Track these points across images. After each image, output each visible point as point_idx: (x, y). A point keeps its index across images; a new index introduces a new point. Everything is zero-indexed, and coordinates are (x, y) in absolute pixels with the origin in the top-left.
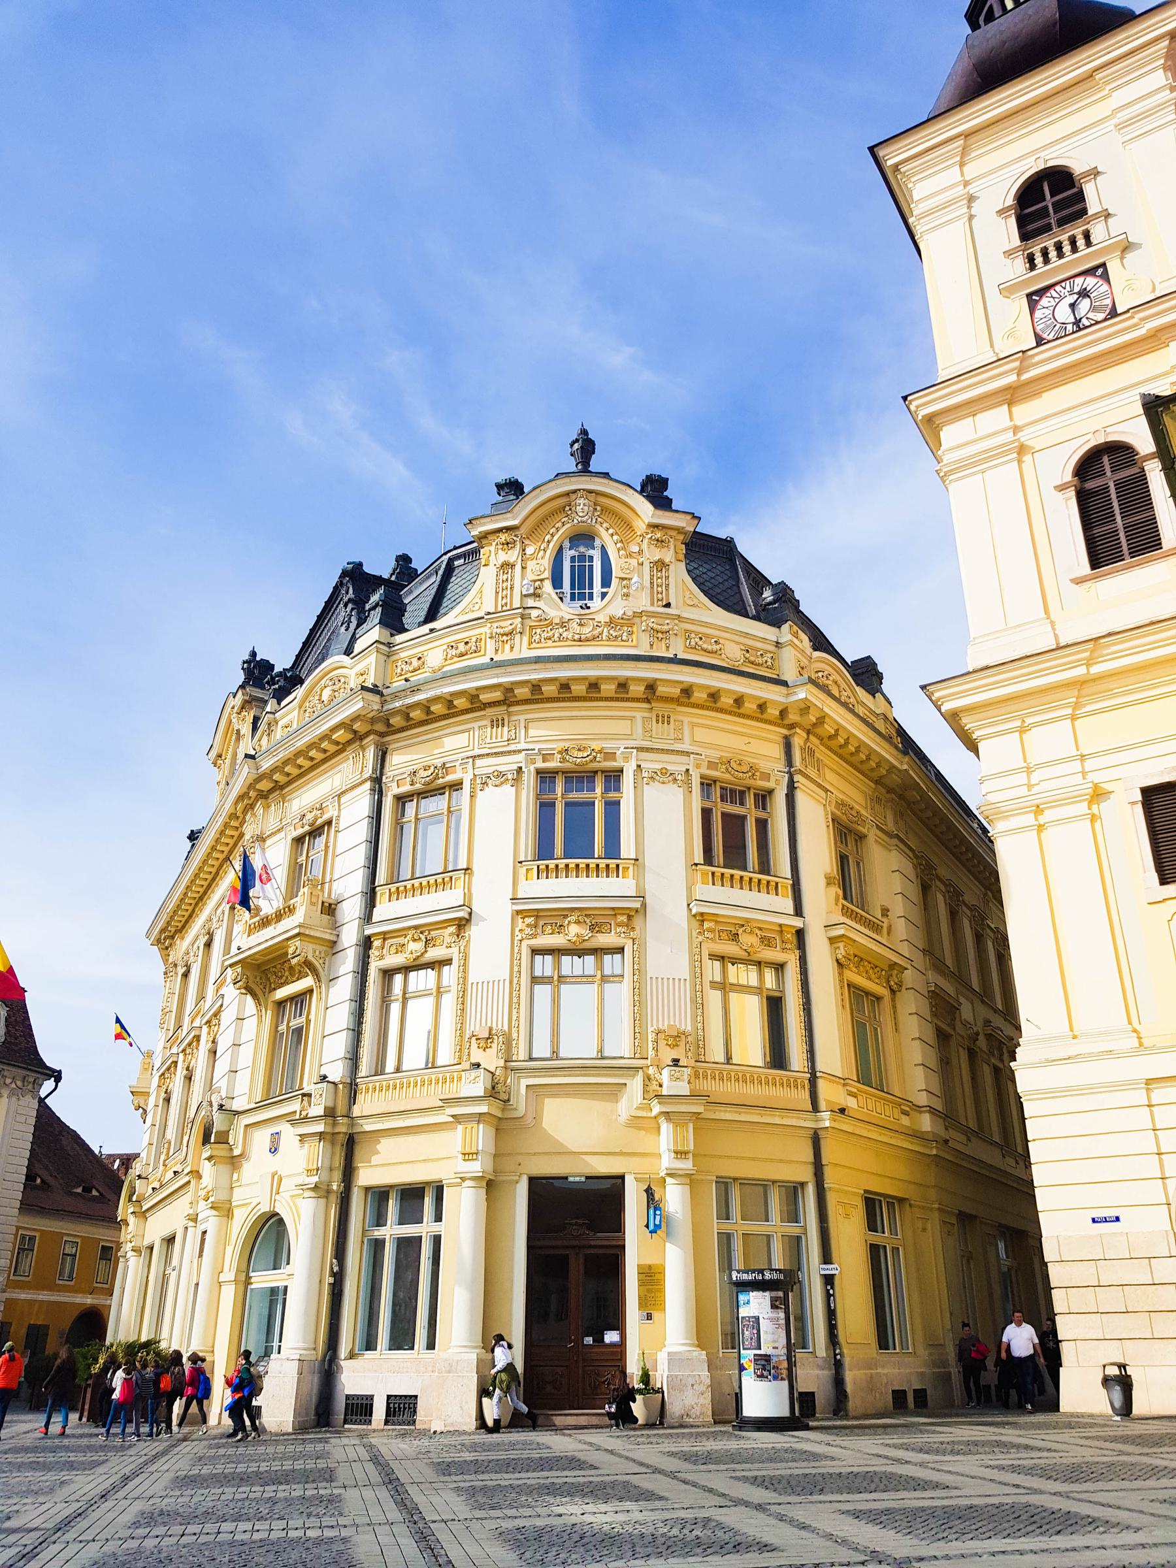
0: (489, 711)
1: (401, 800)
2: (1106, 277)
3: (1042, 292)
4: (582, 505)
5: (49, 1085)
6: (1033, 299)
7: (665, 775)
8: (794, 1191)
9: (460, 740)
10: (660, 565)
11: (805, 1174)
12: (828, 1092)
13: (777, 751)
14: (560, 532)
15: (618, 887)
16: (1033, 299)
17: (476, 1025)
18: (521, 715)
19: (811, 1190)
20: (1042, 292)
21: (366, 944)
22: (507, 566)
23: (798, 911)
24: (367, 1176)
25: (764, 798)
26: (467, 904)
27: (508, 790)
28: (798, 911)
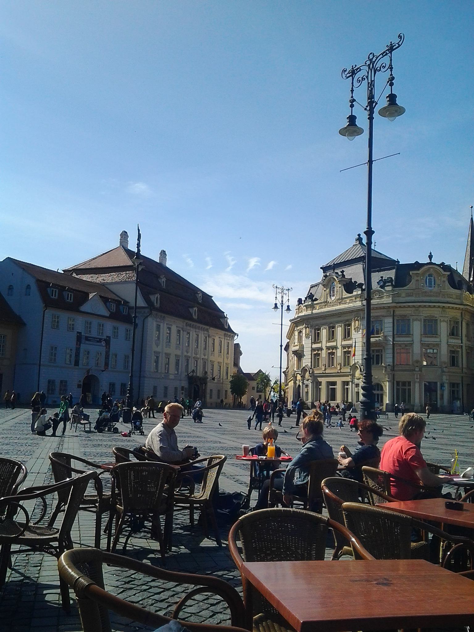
1: (397, 320)
7: (444, 321)
8: (458, 384)
10: (444, 281)
11: (460, 382)
12: (464, 370)
13: (460, 315)
15: (438, 340)
17: (415, 359)
19: (461, 385)
22: (417, 280)
23: (462, 343)
24: (396, 380)
25: (457, 323)
26: (413, 341)
27: (419, 322)
28: (462, 343)
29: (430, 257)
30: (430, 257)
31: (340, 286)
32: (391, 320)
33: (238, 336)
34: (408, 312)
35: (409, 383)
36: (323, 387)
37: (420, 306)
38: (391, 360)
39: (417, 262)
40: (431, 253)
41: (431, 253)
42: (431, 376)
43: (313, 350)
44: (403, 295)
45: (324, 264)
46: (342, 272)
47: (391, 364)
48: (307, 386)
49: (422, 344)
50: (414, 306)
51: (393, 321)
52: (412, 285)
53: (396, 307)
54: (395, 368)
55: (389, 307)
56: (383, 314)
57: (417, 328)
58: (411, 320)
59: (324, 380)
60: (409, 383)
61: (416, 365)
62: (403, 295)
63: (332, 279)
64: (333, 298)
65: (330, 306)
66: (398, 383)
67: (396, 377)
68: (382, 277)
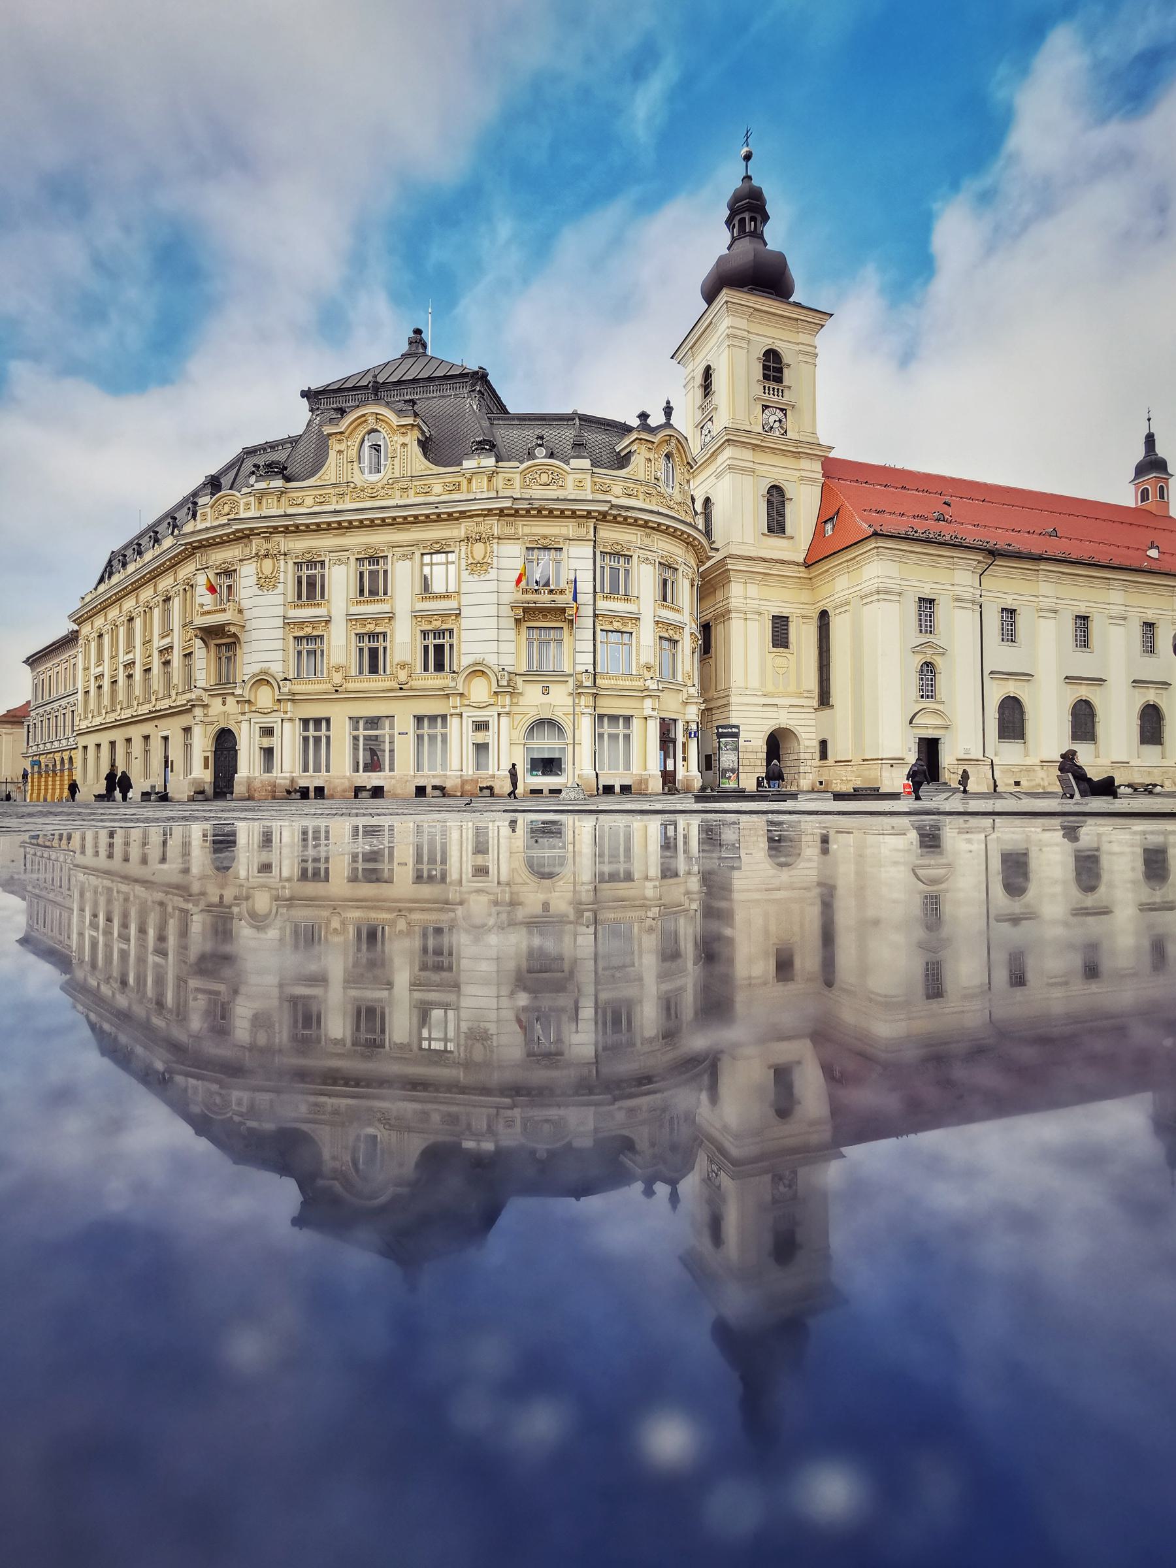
0: (647, 530)
2: (785, 415)
3: (767, 407)
4: (673, 442)
6: (765, 407)
9: (632, 538)
14: (665, 450)
16: (765, 407)
17: (642, 661)
18: (656, 536)
20: (767, 407)
21: (595, 616)
27: (650, 567)
29: (668, 411)
30: (668, 411)
31: (407, 440)
32: (588, 550)
34: (627, 537)
35: (628, 719)
36: (341, 735)
37: (658, 528)
38: (589, 658)
39: (644, 416)
40: (668, 402)
41: (668, 402)
42: (671, 705)
43: (287, 624)
44: (617, 489)
45: (316, 384)
46: (413, 402)
47: (591, 669)
48: (268, 732)
49: (657, 622)
50: (646, 525)
51: (594, 553)
52: (638, 466)
53: (603, 517)
54: (599, 682)
55: (589, 515)
56: (564, 531)
57: (645, 579)
58: (635, 557)
59: (340, 715)
60: (628, 719)
61: (648, 675)
62: (617, 489)
63: (371, 419)
64: (374, 478)
65: (363, 500)
66: (601, 717)
67: (601, 702)
68: (542, 438)
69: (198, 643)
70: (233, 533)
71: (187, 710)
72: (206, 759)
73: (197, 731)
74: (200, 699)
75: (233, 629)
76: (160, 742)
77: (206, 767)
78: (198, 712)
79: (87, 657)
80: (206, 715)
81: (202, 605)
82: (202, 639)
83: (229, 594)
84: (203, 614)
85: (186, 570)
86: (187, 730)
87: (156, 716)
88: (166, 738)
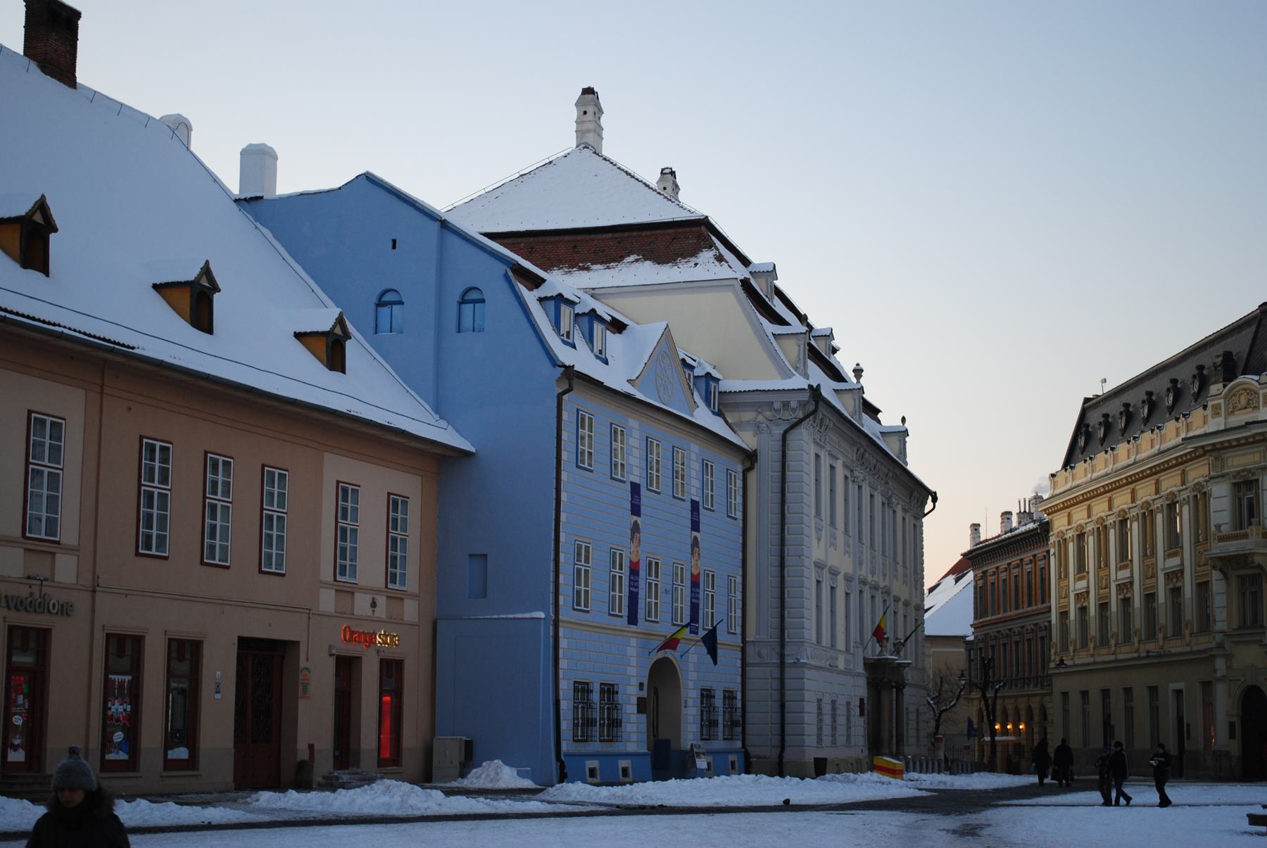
5: (929, 505)
33: (935, 500)
69: (1216, 575)
70: (1253, 436)
71: (1207, 658)
72: (1232, 725)
73: (1221, 691)
74: (1220, 646)
75: (1258, 560)
76: (1171, 699)
77: (1232, 735)
78: (1220, 664)
79: (1063, 564)
80: (1229, 668)
81: (1218, 527)
82: (1221, 570)
83: (1251, 515)
84: (1221, 539)
85: (1198, 472)
86: (1207, 686)
87: (1162, 661)
88: (1179, 693)
